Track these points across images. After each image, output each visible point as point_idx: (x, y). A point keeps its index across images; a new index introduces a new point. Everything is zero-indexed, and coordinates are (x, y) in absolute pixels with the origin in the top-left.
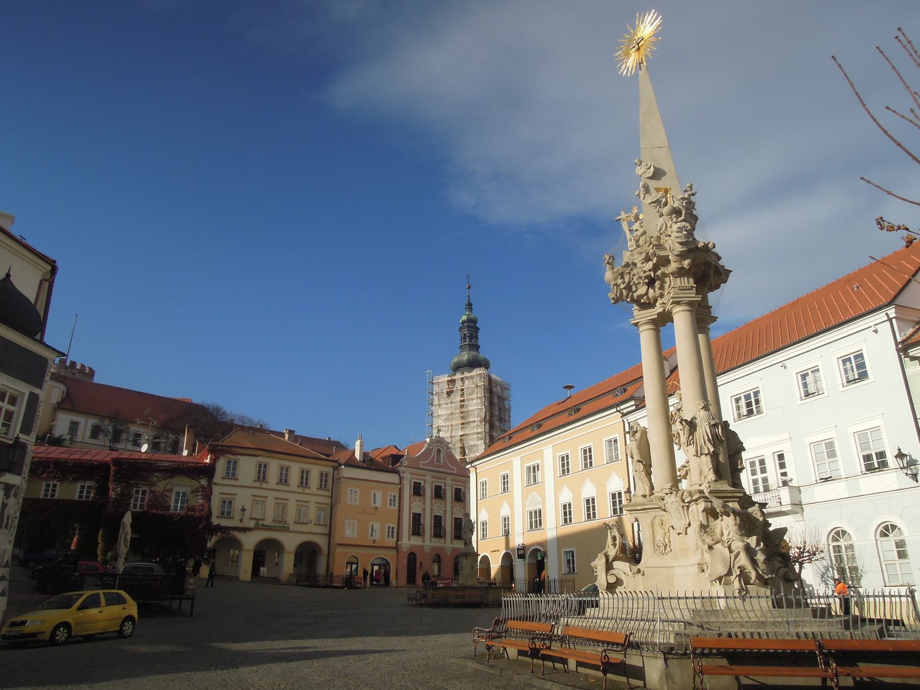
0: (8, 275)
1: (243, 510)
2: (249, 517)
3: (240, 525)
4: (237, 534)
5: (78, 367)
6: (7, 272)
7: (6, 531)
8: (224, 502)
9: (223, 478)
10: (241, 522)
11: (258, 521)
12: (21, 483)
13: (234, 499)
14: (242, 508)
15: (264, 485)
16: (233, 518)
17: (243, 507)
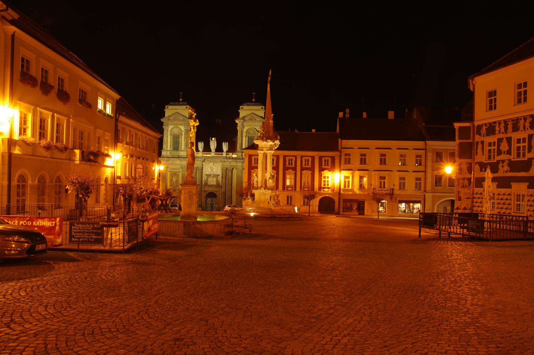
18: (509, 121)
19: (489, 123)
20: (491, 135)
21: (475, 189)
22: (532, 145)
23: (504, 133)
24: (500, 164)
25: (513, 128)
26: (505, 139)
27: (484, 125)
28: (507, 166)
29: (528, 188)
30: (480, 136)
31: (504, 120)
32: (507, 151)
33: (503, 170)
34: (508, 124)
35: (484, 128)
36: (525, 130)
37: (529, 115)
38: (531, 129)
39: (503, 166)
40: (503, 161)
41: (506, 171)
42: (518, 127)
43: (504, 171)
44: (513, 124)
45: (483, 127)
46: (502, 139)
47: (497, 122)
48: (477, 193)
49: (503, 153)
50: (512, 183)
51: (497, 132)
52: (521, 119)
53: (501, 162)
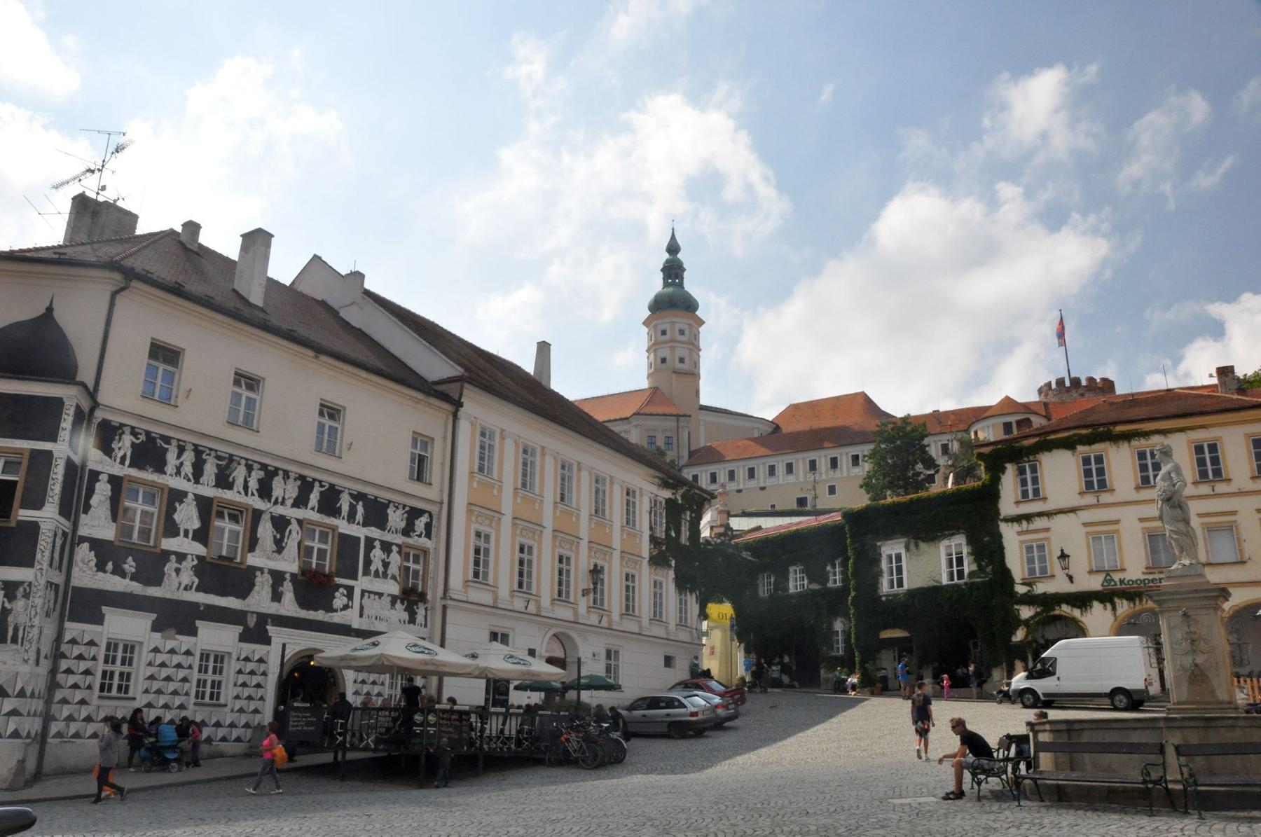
0: (50, 309)
1: (1063, 556)
2: (1088, 570)
3: (1072, 588)
4: (1066, 609)
5: (1084, 383)
6: (48, 304)
7: (14, 647)
8: (1029, 549)
9: (1017, 503)
10: (1072, 582)
11: (1108, 575)
12: (36, 577)
13: (1047, 539)
14: (1059, 554)
15: (1105, 498)
16: (1053, 576)
17: (1062, 551)
18: (209, 455)
19: (148, 433)
20: (151, 469)
21: (68, 625)
22: (259, 536)
23: (189, 480)
24: (169, 560)
25: (217, 476)
26: (191, 496)
27: (127, 430)
28: (192, 573)
29: (240, 640)
30: (111, 457)
31: (196, 446)
32: (195, 531)
33: (177, 580)
34: (205, 461)
35: (128, 439)
36: (246, 494)
37: (259, 463)
38: (259, 496)
39: (178, 571)
40: (181, 557)
41: (186, 586)
42: (231, 479)
43: (180, 584)
44: (218, 465)
45: (123, 433)
46: (185, 494)
47: (174, 443)
48: (73, 642)
49: (182, 533)
50: (198, 623)
51: (170, 468)
52: (239, 464)
53: (173, 558)
